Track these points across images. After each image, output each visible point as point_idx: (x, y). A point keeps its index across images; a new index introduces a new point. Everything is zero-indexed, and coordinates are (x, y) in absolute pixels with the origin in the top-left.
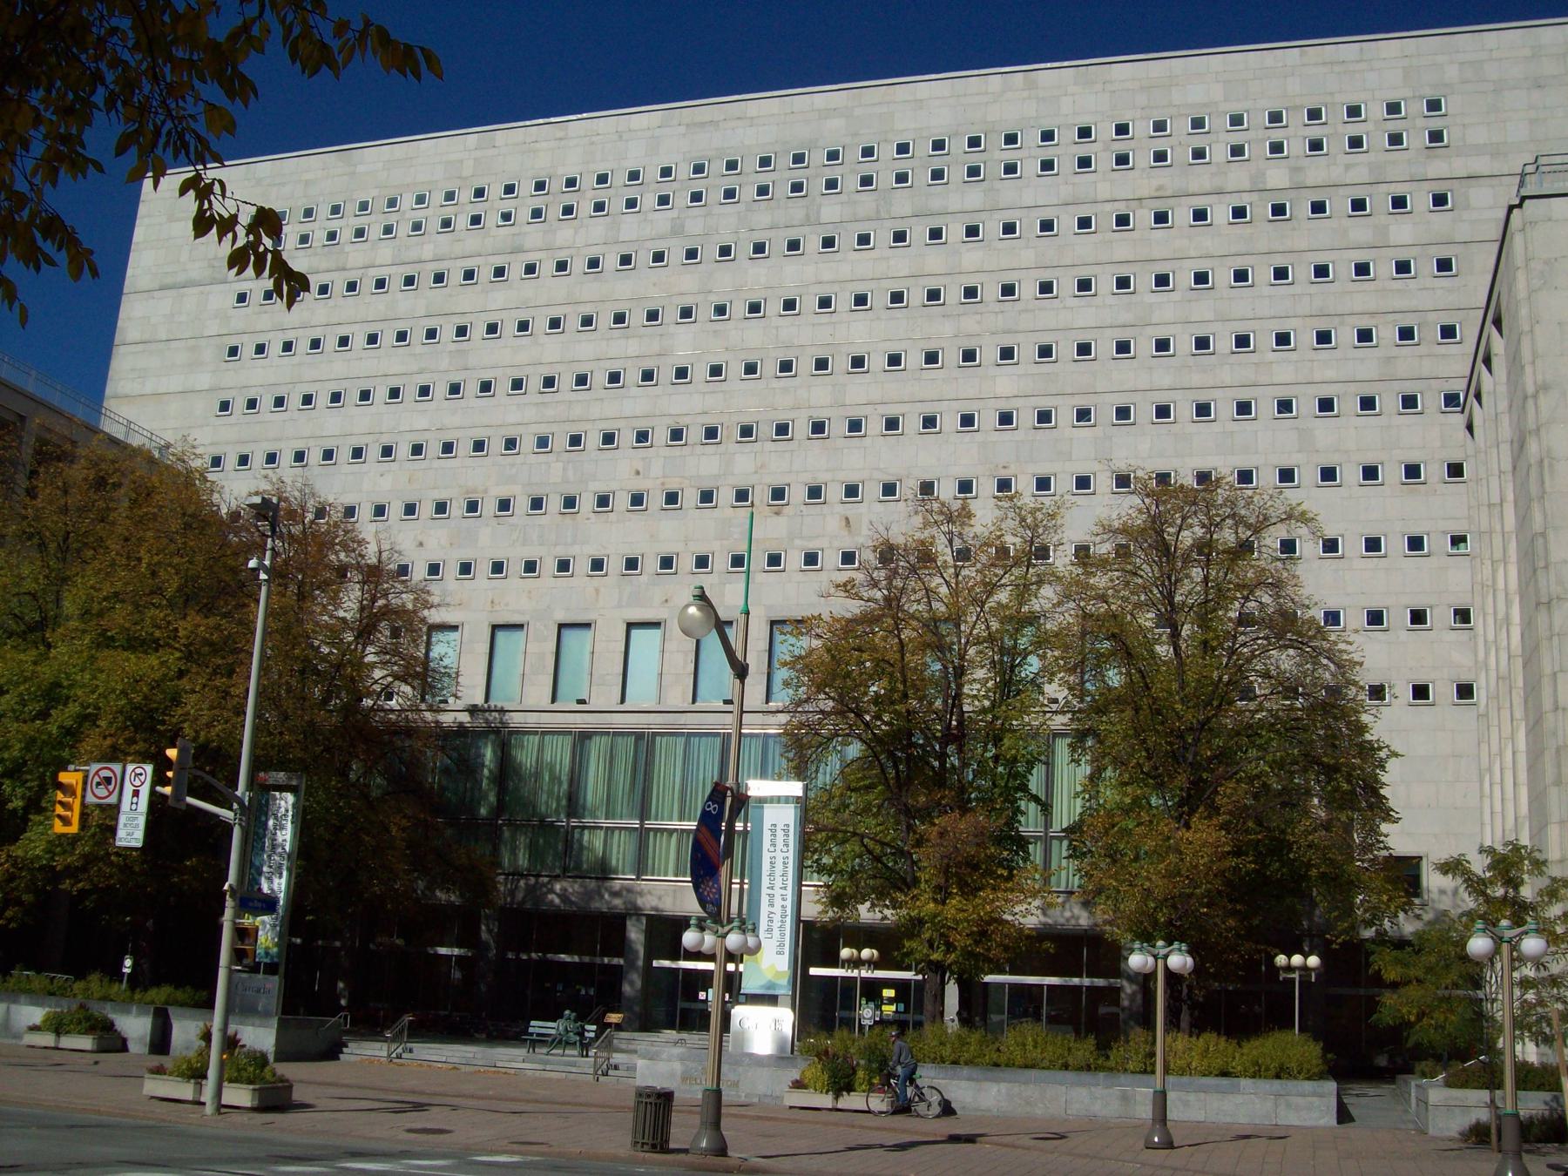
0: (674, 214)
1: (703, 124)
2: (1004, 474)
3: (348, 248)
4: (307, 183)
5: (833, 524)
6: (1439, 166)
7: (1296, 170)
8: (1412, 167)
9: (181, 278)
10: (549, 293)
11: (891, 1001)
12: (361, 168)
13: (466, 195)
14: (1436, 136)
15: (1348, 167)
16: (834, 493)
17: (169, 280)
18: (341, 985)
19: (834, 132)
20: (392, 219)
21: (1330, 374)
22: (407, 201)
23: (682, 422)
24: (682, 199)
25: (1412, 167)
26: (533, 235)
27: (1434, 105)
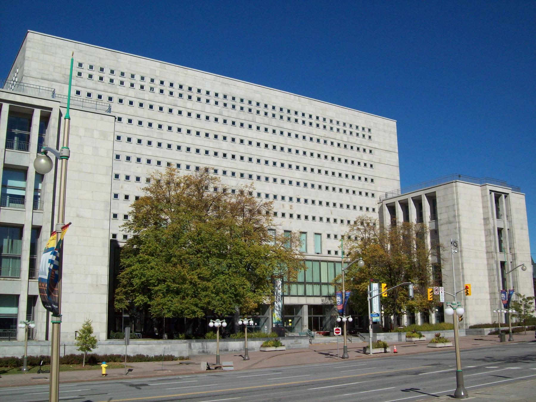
0: (220, 108)
1: (225, 84)
2: (298, 197)
3: (118, 87)
4: (100, 58)
6: (371, 144)
7: (348, 138)
8: (364, 143)
9: (51, 77)
10: (185, 122)
11: (291, 322)
12: (119, 60)
13: (157, 82)
14: (370, 137)
15: (357, 140)
17: (45, 77)
18: (156, 329)
19: (256, 98)
20: (133, 82)
22: (138, 77)
23: (226, 169)
24: (221, 104)
25: (364, 143)
26: (180, 102)
27: (369, 130)
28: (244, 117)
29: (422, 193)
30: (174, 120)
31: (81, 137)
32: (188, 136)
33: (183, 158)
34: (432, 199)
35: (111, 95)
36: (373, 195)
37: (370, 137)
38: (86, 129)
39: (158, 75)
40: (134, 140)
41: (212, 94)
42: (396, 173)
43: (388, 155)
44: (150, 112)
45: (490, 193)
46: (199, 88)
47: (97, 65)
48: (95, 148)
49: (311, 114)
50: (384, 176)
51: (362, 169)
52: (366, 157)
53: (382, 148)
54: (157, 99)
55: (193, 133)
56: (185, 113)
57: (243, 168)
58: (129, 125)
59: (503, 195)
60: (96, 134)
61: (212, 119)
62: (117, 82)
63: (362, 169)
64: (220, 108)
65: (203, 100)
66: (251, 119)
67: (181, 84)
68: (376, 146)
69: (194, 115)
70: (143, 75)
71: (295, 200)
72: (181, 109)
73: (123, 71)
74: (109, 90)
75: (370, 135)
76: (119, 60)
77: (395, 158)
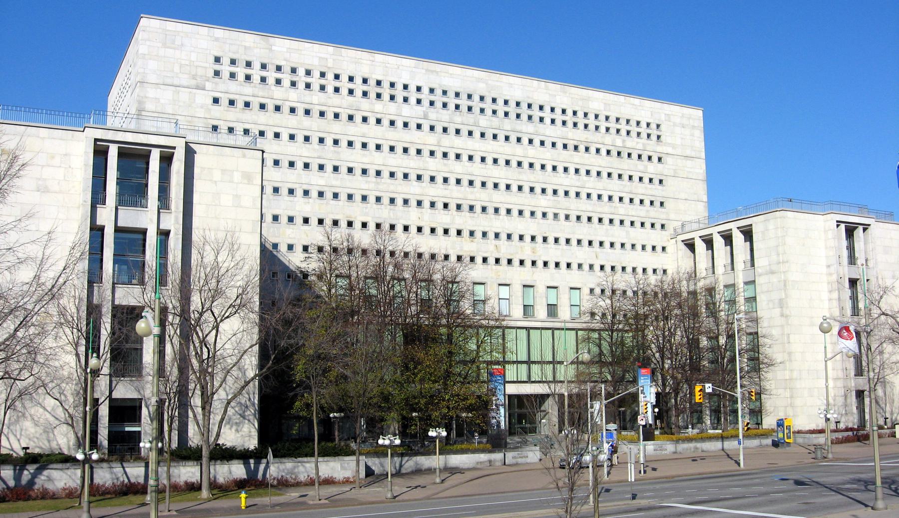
0: (424, 109)
1: (432, 71)
4: (245, 47)
5: (492, 248)
6: (661, 149)
8: (652, 148)
9: (176, 82)
13: (330, 76)
15: (637, 143)
16: (491, 235)
17: (169, 81)
19: (479, 89)
21: (634, 213)
23: (435, 199)
27: (658, 126)
28: (461, 120)
29: (733, 226)
30: (356, 131)
31: (216, 182)
32: (377, 154)
33: (372, 186)
34: (748, 234)
35: (263, 101)
36: (663, 226)
37: (659, 137)
38: (224, 171)
39: (330, 65)
40: (299, 165)
41: (412, 88)
42: (701, 191)
43: (689, 163)
44: (322, 121)
45: (838, 226)
46: (393, 80)
47: (242, 58)
48: (237, 197)
49: (564, 107)
50: (683, 196)
51: (646, 188)
52: (653, 169)
53: (679, 151)
54: (330, 102)
55: (386, 148)
56: (372, 121)
57: (460, 196)
58: (292, 144)
59: (861, 228)
60: (237, 177)
61: (412, 125)
62: (271, 81)
63: (646, 188)
64: (424, 109)
65: (399, 99)
66: (471, 121)
67: (366, 76)
68: (669, 150)
69: (386, 122)
70: (309, 68)
71: (539, 239)
72: (365, 114)
73: (279, 64)
74: (261, 94)
75: (659, 133)
76: (274, 48)
77: (699, 168)
